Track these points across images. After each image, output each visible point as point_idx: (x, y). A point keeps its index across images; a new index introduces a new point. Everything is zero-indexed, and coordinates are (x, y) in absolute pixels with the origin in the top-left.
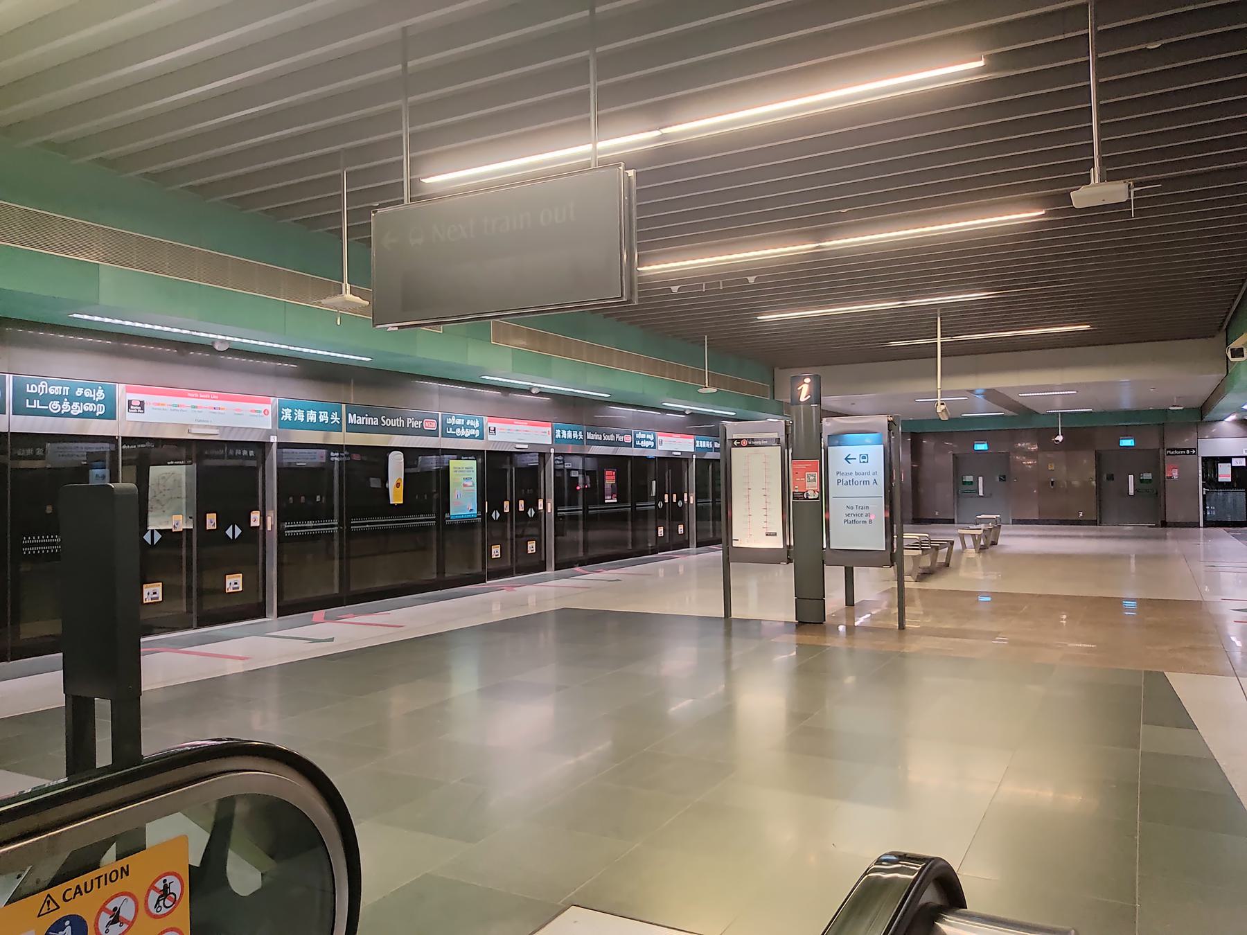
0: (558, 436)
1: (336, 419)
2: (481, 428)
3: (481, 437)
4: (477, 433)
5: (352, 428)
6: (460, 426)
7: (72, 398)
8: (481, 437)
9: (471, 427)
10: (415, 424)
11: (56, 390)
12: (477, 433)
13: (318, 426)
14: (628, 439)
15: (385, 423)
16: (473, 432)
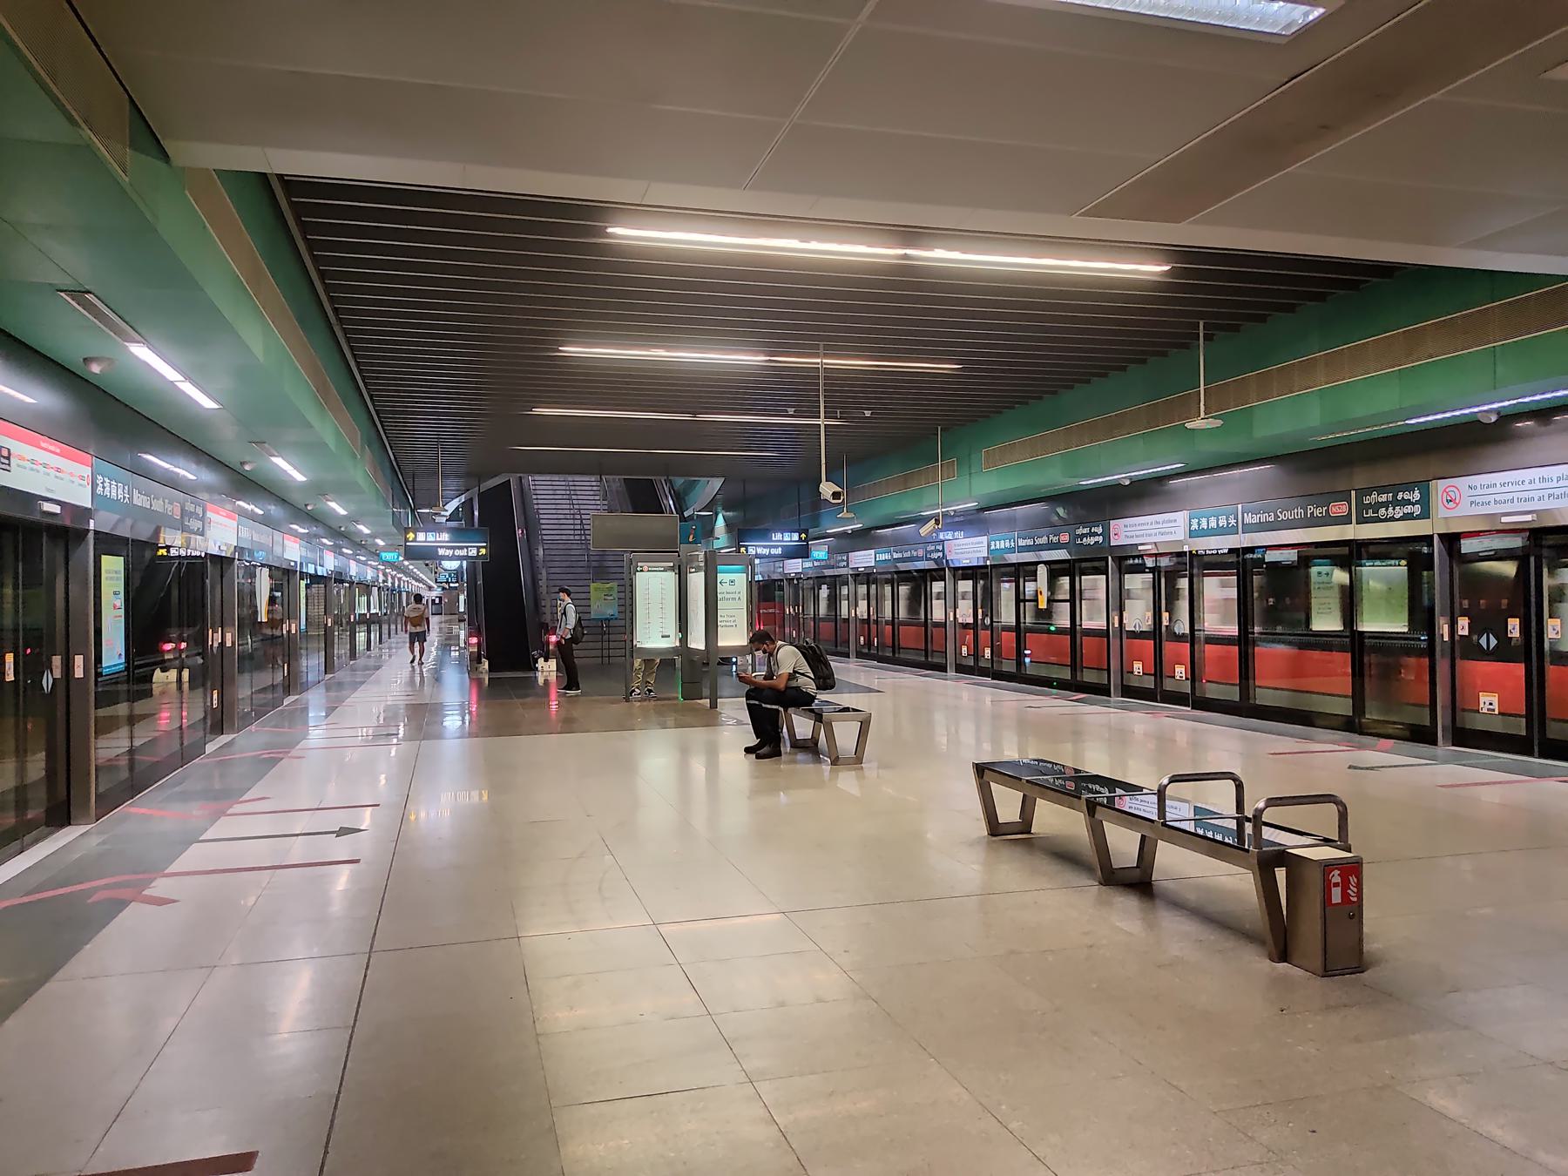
0: (1195, 526)
1: (1233, 522)
2: (1425, 502)
3: (1425, 514)
4: (1417, 510)
5: (1248, 529)
6: (1385, 505)
7: (1396, 503)
8: (1425, 514)
9: (1409, 502)
10: (1317, 513)
11: (1383, 498)
12: (1417, 510)
13: (1027, 549)
14: (921, 553)
15: (1282, 517)
16: (1408, 509)
